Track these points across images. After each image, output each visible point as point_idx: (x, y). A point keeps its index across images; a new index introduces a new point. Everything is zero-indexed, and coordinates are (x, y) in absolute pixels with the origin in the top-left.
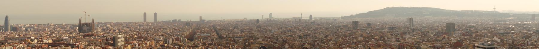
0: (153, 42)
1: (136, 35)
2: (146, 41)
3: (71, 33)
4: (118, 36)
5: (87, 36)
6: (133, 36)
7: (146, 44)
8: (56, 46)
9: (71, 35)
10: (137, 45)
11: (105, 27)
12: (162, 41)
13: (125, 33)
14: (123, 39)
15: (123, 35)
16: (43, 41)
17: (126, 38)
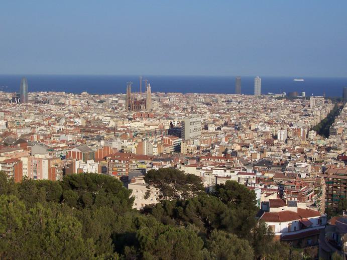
4: (191, 120)
10: (224, 139)
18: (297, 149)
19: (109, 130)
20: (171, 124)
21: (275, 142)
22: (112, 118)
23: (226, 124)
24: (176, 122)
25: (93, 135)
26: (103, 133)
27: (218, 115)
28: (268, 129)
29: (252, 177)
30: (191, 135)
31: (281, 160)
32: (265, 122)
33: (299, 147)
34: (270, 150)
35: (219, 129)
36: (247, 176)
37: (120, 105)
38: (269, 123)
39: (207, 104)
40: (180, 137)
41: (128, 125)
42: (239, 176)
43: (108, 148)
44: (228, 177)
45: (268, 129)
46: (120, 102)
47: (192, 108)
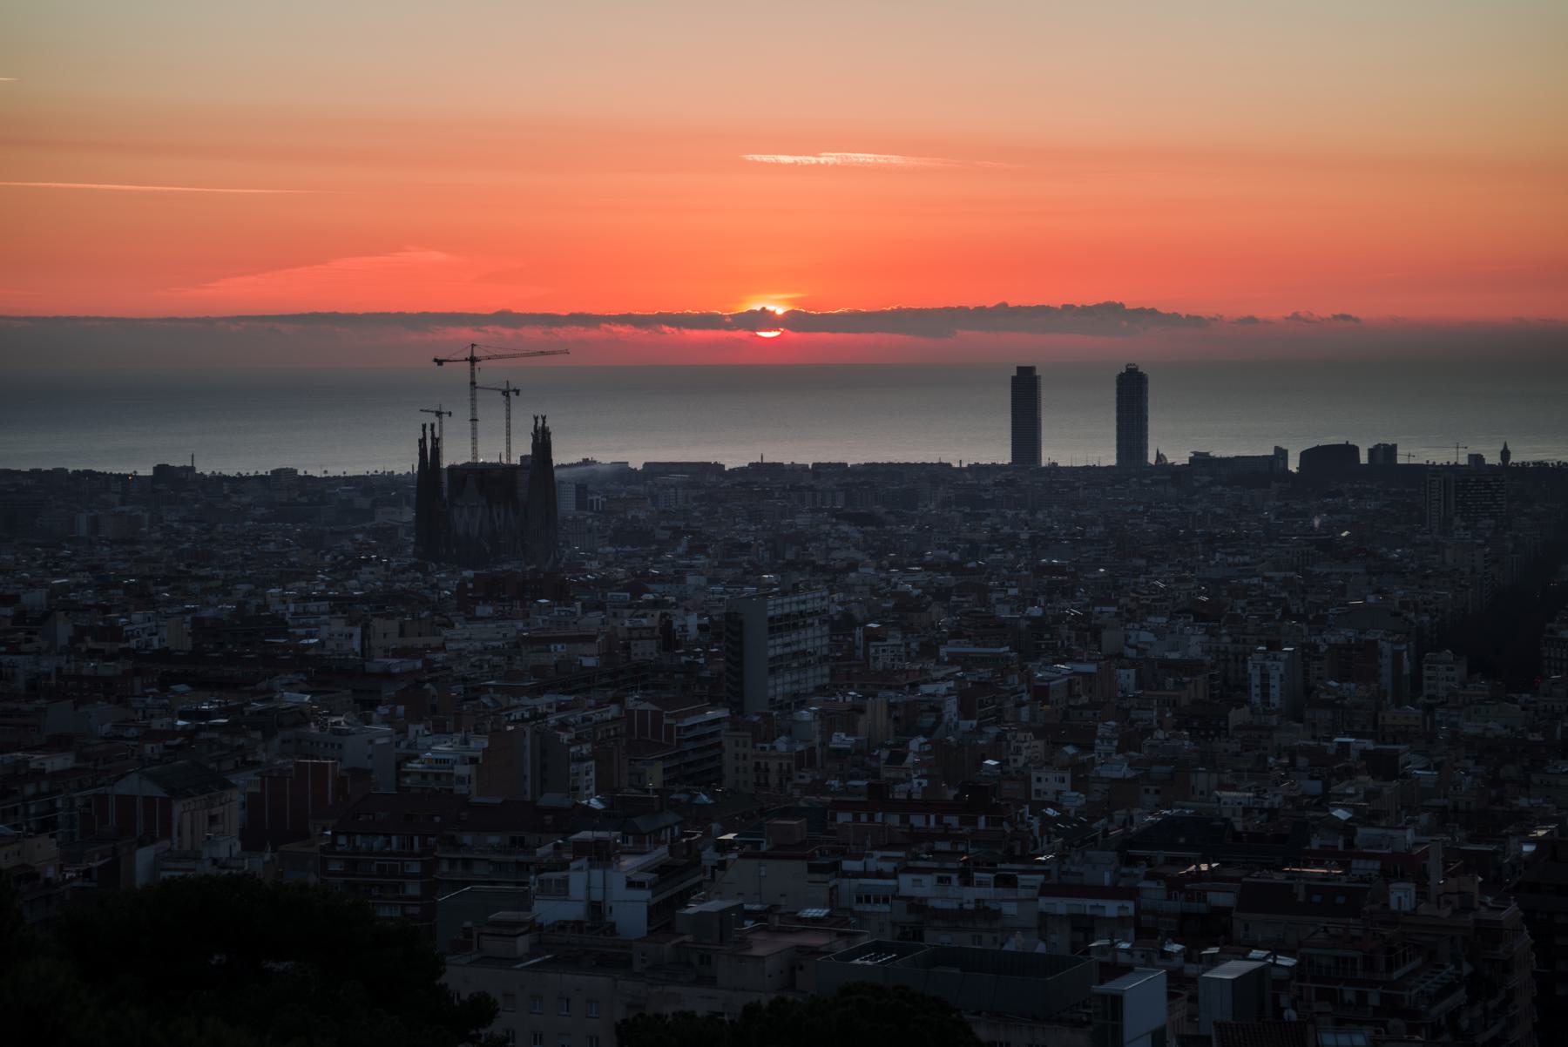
10: (951, 706)
16: (115, 633)
18: (1364, 754)
19: (326, 674)
21: (1237, 716)
28: (1195, 643)
29: (1111, 908)
30: (780, 686)
31: (1272, 812)
33: (1369, 745)
35: (929, 651)
36: (1087, 905)
38: (1200, 617)
39: (858, 520)
41: (435, 641)
42: (1044, 903)
45: (1195, 643)
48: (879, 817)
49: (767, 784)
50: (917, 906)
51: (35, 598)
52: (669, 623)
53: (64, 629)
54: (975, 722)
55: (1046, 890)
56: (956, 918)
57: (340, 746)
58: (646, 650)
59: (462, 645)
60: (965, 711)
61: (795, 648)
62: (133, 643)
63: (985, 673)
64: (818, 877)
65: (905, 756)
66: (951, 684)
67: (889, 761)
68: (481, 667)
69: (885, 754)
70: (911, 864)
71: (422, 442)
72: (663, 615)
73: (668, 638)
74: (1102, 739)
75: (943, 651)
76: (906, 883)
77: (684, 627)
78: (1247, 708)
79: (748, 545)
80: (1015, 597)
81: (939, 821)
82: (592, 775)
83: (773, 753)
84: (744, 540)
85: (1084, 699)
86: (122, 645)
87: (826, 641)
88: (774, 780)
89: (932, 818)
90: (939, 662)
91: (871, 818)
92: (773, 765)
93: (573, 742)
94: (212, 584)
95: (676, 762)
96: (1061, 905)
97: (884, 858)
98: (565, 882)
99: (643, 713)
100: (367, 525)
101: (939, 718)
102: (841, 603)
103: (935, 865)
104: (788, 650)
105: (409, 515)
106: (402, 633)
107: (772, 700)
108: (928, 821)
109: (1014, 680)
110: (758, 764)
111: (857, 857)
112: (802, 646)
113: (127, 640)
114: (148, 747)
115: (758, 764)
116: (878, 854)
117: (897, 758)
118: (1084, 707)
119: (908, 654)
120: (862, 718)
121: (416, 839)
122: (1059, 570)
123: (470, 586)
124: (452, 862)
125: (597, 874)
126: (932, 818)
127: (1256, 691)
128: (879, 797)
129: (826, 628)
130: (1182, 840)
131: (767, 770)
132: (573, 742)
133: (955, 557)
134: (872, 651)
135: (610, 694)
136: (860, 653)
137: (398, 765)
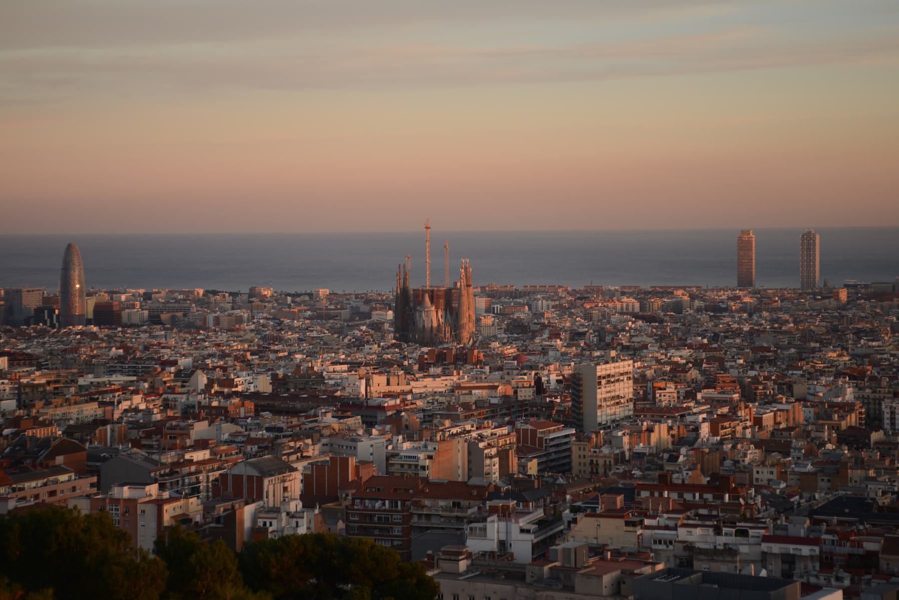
0: (801, 413)
1: (697, 364)
2: (754, 407)
3: (359, 344)
4: (602, 370)
5: (440, 359)
6: (677, 372)
7: (758, 422)
8: (295, 413)
9: (359, 357)
10: (705, 429)
11: (523, 314)
12: (847, 408)
13: (633, 351)
14: (626, 389)
15: (627, 365)
17: (640, 380)
20: (538, 381)
21: (875, 436)
22: (354, 366)
23: (710, 383)
24: (553, 377)
25: (295, 421)
26: (329, 419)
27: (686, 352)
29: (805, 550)
32: (838, 374)
34: (860, 464)
36: (791, 548)
37: (377, 327)
38: (852, 377)
39: (649, 319)
40: (567, 425)
42: (765, 547)
43: (345, 462)
44: (730, 552)
46: (376, 316)
47: (601, 333)
48: (666, 494)
49: (597, 472)
50: (689, 547)
51: (184, 362)
52: (540, 379)
53: (202, 379)
54: (719, 438)
55: (766, 539)
56: (713, 554)
57: (355, 448)
58: (526, 394)
59: (422, 391)
60: (714, 431)
61: (613, 394)
62: (240, 389)
63: (725, 410)
64: (631, 529)
65: (678, 458)
66: (705, 416)
67: (668, 460)
68: (433, 403)
69: (666, 456)
70: (685, 522)
71: (398, 275)
72: (536, 374)
73: (539, 387)
74: (795, 449)
75: (699, 396)
76: (682, 534)
77: (548, 381)
78: (881, 432)
79: (584, 334)
80: (741, 365)
81: (701, 497)
82: (497, 466)
83: (601, 455)
84: (581, 330)
85: (783, 426)
86: (234, 390)
87: (631, 390)
88: (601, 470)
89: (697, 495)
90: (698, 403)
91: (661, 495)
92: (601, 462)
93: (486, 448)
94: (281, 354)
95: (544, 459)
96: (776, 548)
97: (669, 518)
98: (485, 529)
99: (526, 431)
100: (368, 321)
101: (698, 435)
102: (639, 368)
103: (700, 523)
104: (609, 395)
105: (390, 314)
106: (388, 384)
107: (600, 424)
108: (694, 497)
109: (742, 413)
110: (592, 461)
111: (654, 517)
112: (617, 393)
113: (236, 386)
114: (249, 448)
115: (592, 461)
116: (665, 516)
117: (674, 458)
118: (783, 429)
119: (678, 398)
120: (652, 434)
121: (399, 503)
122: (768, 349)
123: (426, 356)
124: (420, 516)
125: (503, 525)
126: (697, 495)
127: (887, 422)
128: (665, 482)
129: (631, 382)
130: (847, 511)
131: (597, 464)
132: (486, 448)
133: (705, 341)
134: (658, 395)
135: (507, 419)
136: (650, 397)
137: (387, 459)
